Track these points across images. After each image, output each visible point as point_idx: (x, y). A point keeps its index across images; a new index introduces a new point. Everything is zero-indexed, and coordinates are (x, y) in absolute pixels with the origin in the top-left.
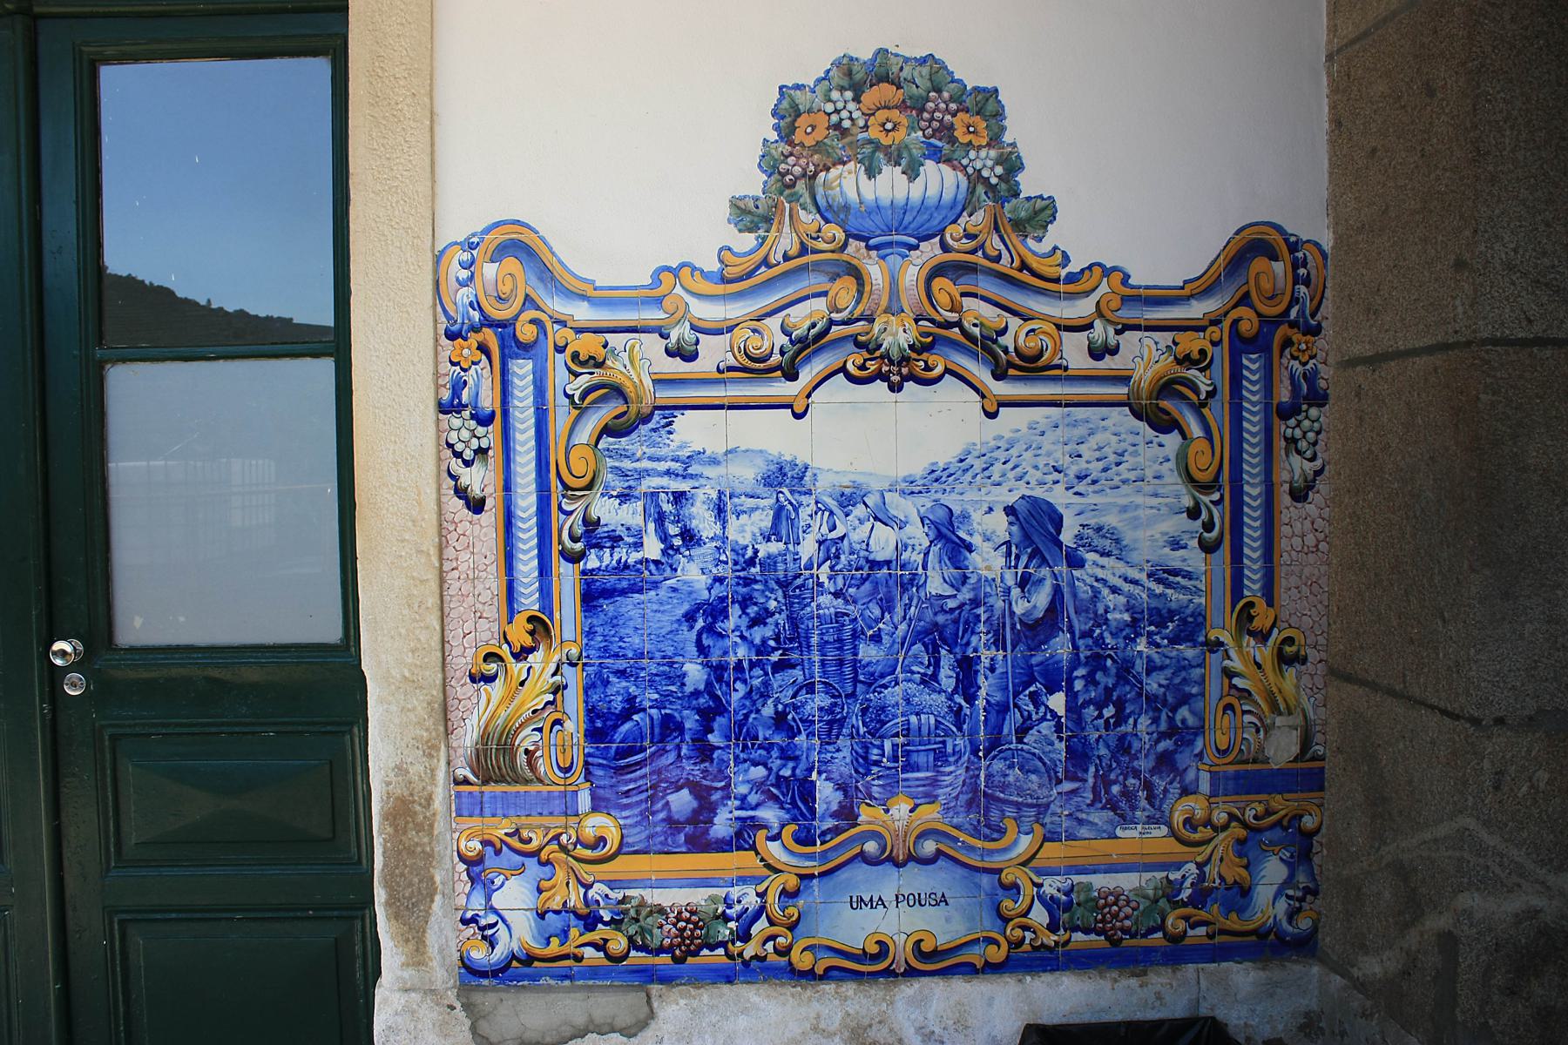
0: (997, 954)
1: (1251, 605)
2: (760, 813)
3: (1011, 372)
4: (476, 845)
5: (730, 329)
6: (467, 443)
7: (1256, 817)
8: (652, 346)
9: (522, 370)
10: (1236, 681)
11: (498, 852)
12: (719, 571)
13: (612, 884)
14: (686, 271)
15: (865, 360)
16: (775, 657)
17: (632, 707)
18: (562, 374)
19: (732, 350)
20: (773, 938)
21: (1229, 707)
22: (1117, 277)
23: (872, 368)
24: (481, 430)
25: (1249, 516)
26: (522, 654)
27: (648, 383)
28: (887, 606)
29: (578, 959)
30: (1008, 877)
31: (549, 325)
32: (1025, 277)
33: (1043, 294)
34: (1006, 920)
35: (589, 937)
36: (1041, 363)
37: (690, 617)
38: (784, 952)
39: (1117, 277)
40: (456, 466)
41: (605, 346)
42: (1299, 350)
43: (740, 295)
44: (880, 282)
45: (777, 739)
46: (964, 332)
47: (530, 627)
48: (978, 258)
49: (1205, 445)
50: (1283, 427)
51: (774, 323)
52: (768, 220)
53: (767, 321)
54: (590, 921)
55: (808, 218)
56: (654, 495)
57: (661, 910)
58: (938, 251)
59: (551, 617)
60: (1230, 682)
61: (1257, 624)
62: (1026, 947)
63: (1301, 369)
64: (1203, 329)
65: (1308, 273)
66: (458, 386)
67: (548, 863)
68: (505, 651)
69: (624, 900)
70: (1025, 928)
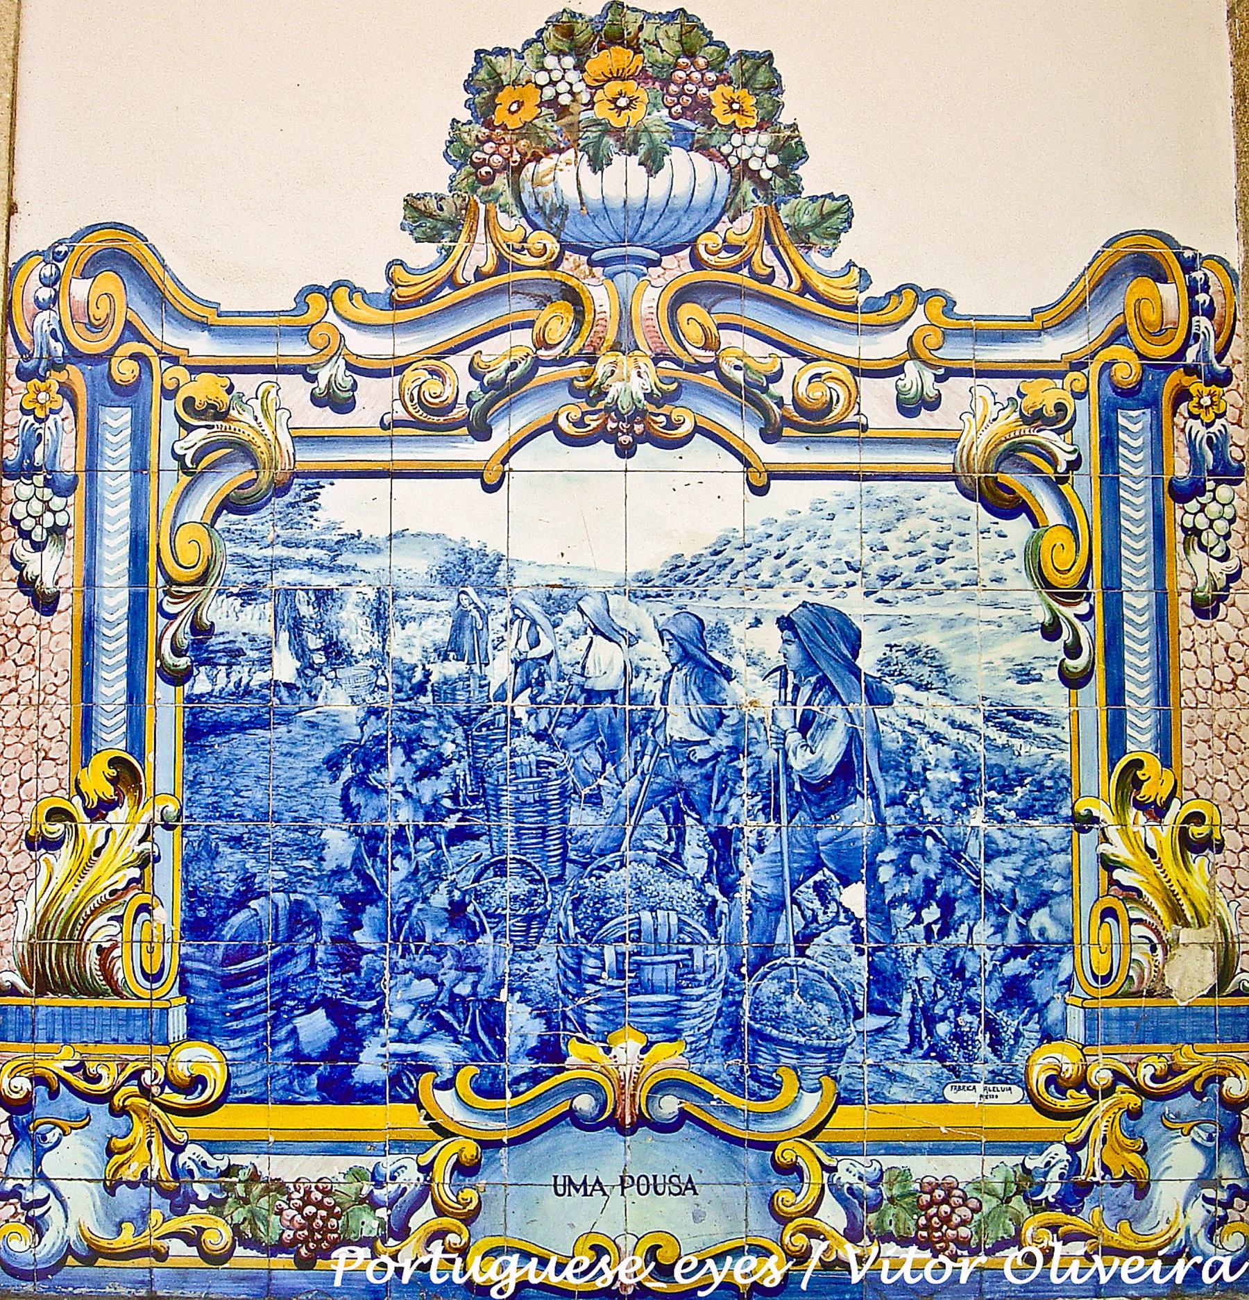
1: (1138, 764)
2: (425, 1048)
3: (787, 431)
4: (24, 1084)
5: (400, 370)
6: (38, 520)
7: (1154, 1078)
8: (295, 390)
9: (117, 420)
10: (1118, 874)
11: (54, 1094)
12: (377, 700)
13: (212, 1147)
14: (343, 292)
15: (584, 414)
16: (451, 823)
17: (248, 891)
18: (171, 426)
19: (402, 398)
20: (440, 1234)
22: (937, 304)
23: (594, 424)
24: (57, 503)
25: (1133, 638)
26: (99, 811)
27: (285, 440)
28: (611, 755)
29: (161, 1256)
30: (785, 1154)
31: (155, 362)
32: (808, 303)
33: (830, 325)
35: (177, 1224)
36: (828, 421)
37: (333, 764)
39: (937, 304)
40: (22, 549)
41: (230, 390)
42: (1200, 406)
43: (415, 324)
44: (606, 308)
45: (452, 940)
47: (113, 773)
48: (742, 278)
49: (1065, 537)
50: (1179, 513)
51: (459, 363)
52: (454, 225)
53: (451, 359)
54: (180, 1202)
55: (510, 225)
56: (288, 593)
57: (278, 1187)
58: (687, 267)
59: (141, 758)
60: (1110, 877)
61: (1146, 792)
63: (1203, 432)
64: (1061, 375)
65: (1211, 300)
67: (123, 1112)
69: (231, 1170)
70: (812, 1233)
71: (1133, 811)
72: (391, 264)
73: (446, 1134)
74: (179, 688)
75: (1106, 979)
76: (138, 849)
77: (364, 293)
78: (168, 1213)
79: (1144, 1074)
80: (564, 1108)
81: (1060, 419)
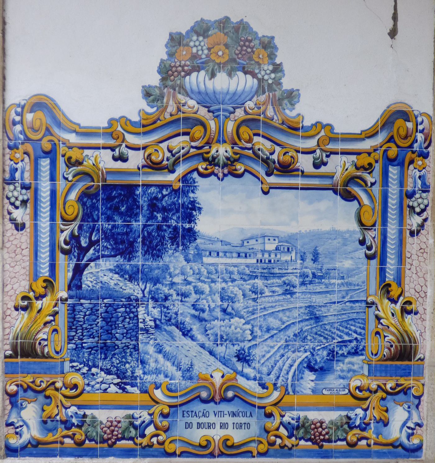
0: (263, 448)
7: (391, 388)
10: (382, 321)
21: (377, 333)
26: (40, 297)
34: (268, 432)
38: (162, 443)
40: (11, 208)
46: (254, 152)
47: (45, 285)
51: (164, 145)
53: (161, 145)
58: (243, 113)
62: (277, 447)
69: (85, 416)
70: (277, 436)
72: (140, 111)
73: (157, 403)
75: (376, 355)
76: (53, 309)
77: (130, 121)
78: (63, 428)
79: (388, 387)
81: (369, 168)
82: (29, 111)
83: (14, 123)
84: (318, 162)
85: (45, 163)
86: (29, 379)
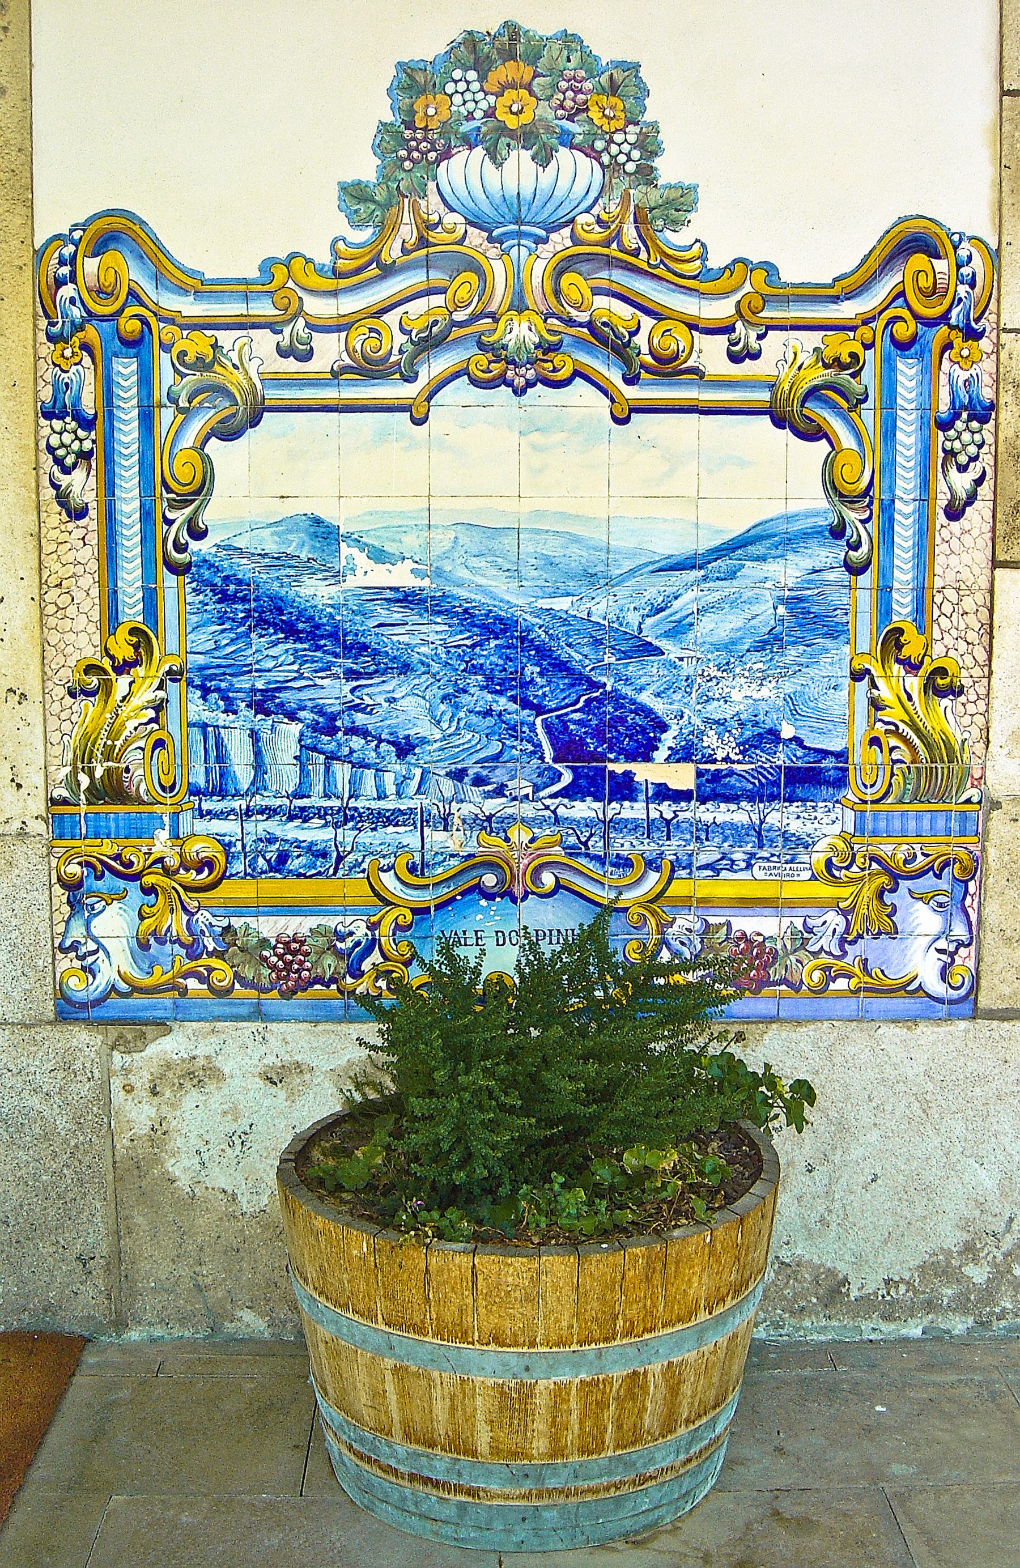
8: (265, 341)
22: (760, 275)
47: (135, 639)
53: (386, 317)
58: (568, 243)
61: (906, 652)
66: (60, 388)
68: (107, 664)
71: (896, 667)
72: (335, 241)
74: (181, 578)
80: (476, 881)
82: (90, 249)
83: (60, 283)
84: (737, 352)
85: (126, 369)
86: (108, 848)
